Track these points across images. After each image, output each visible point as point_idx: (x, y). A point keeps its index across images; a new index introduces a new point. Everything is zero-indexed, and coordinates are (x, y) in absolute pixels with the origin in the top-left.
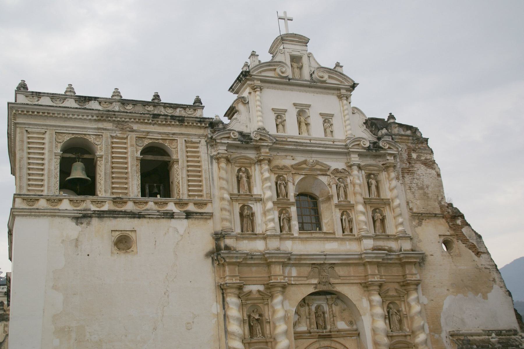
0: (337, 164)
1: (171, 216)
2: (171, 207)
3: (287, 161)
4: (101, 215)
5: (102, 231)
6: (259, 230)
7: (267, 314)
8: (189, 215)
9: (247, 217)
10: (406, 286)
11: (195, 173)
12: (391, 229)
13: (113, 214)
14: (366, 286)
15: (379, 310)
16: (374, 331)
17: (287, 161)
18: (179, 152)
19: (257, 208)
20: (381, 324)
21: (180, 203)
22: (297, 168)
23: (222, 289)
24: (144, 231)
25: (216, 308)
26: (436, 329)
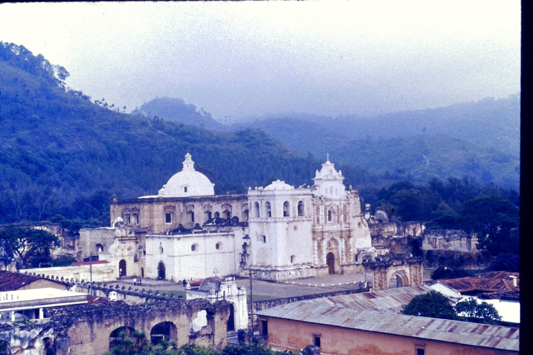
0: (337, 203)
1: (304, 221)
2: (304, 218)
3: (327, 203)
4: (291, 222)
5: (292, 225)
6: (321, 223)
7: (321, 245)
8: (308, 220)
9: (318, 220)
10: (349, 237)
11: (308, 209)
12: (348, 221)
13: (294, 221)
14: (341, 237)
15: (344, 243)
16: (342, 248)
17: (327, 203)
18: (305, 203)
19: (320, 217)
20: (344, 247)
21: (306, 217)
22: (329, 205)
23: (314, 239)
24: (299, 225)
25: (312, 243)
26: (354, 247)
